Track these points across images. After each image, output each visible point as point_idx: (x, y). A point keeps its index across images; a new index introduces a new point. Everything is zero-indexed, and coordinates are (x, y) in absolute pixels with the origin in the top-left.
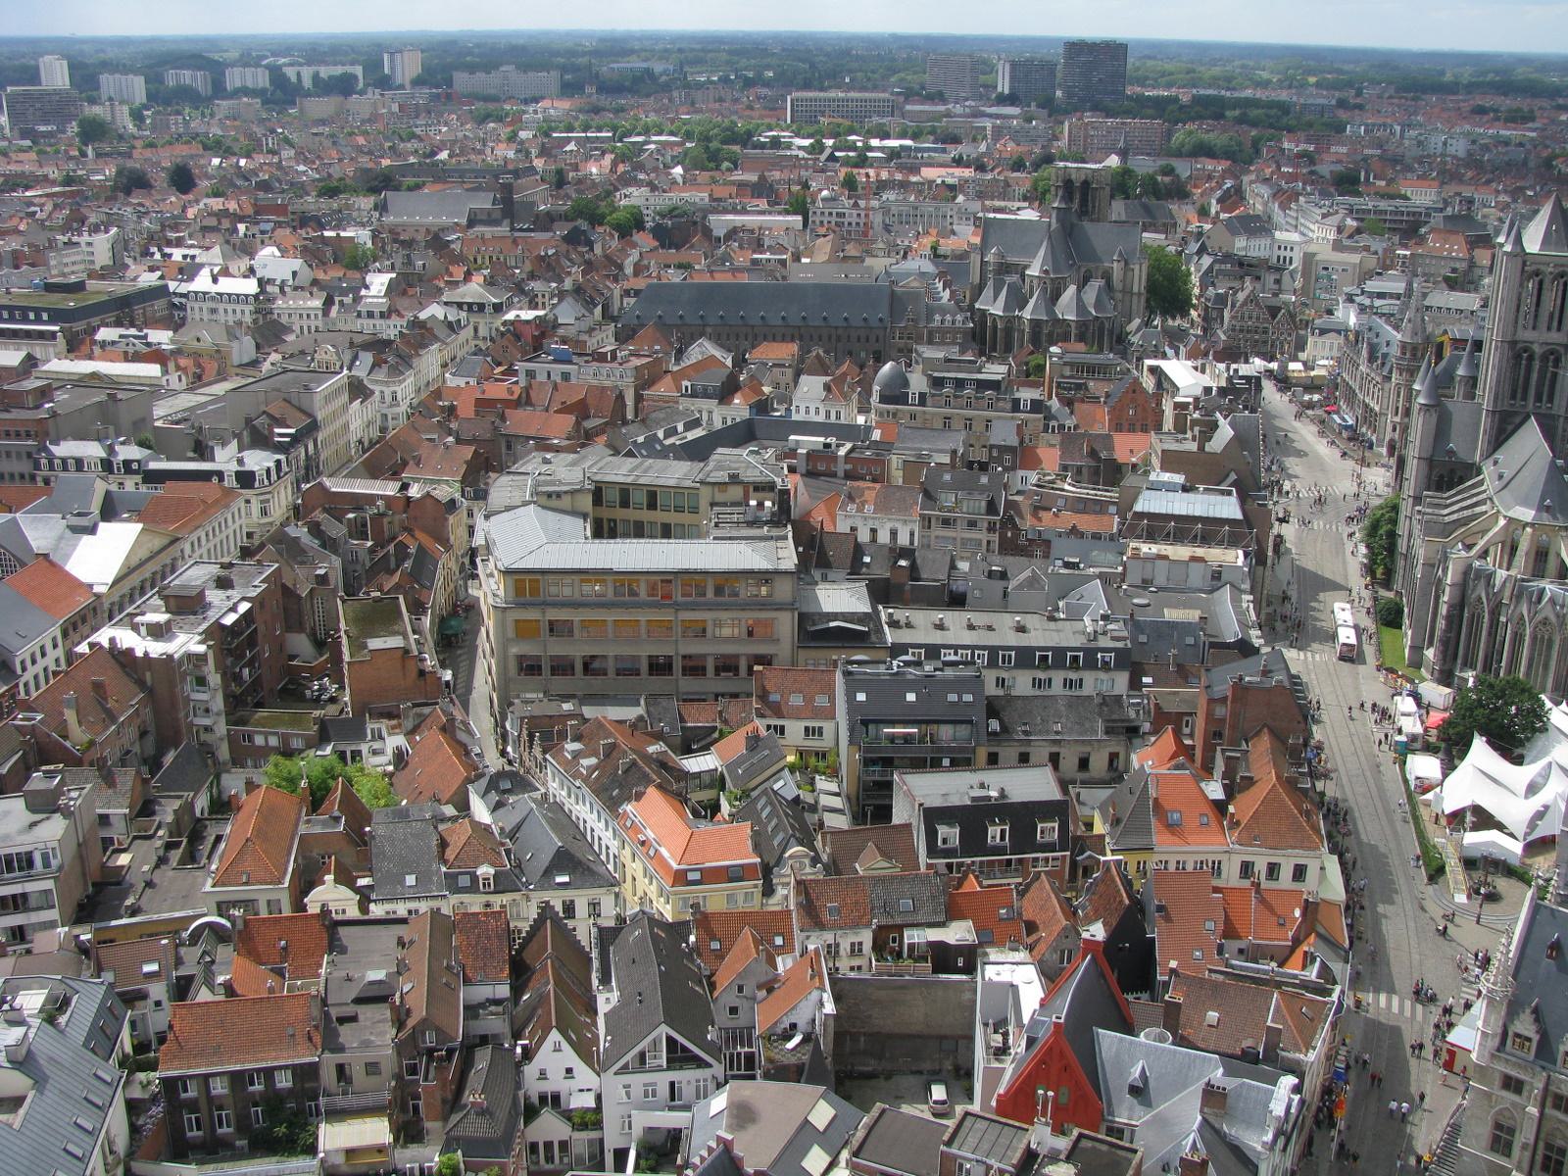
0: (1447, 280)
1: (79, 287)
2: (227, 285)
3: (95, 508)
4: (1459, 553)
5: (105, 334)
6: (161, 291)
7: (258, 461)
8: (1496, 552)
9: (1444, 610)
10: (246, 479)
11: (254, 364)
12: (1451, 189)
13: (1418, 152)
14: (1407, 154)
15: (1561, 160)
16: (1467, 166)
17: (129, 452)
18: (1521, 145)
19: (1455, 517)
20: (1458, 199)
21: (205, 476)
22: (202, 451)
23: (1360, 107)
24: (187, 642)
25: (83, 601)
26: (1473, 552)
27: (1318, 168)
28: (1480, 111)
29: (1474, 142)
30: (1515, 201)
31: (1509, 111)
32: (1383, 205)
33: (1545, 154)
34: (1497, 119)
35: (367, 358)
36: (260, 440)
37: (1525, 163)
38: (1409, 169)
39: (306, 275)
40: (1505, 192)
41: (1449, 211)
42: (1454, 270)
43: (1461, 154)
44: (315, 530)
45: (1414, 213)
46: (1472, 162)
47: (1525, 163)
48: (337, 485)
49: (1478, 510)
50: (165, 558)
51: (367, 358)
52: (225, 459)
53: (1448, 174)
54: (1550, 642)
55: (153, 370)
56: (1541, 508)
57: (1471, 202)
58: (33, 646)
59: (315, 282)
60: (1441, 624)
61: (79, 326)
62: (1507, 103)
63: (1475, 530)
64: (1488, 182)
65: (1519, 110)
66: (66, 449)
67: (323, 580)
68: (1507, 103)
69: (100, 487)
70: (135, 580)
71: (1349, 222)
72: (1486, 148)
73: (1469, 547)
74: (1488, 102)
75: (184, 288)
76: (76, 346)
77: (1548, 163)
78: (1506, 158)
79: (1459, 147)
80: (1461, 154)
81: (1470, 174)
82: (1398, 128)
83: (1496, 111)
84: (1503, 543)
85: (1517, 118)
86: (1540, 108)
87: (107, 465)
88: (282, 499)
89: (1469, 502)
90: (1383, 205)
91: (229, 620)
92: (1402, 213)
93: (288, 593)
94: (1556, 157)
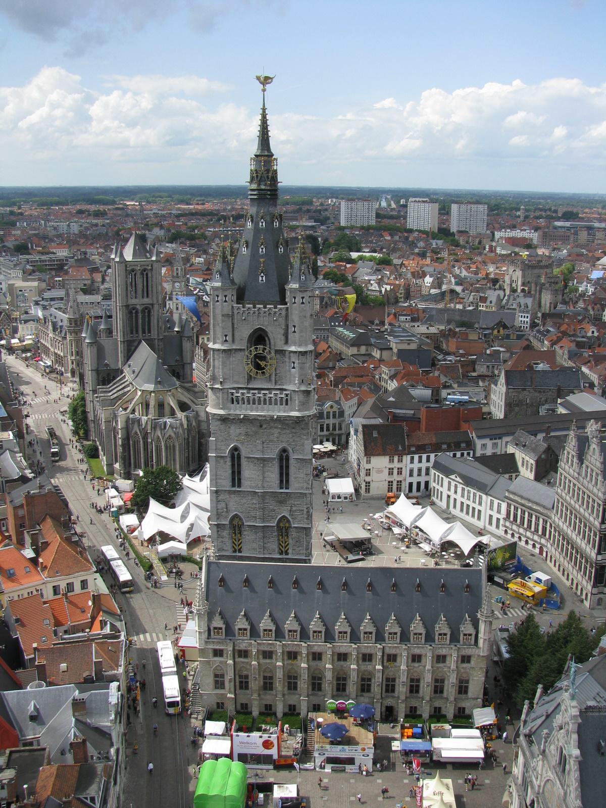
0: (82, 290)
4: (121, 412)
8: (139, 409)
9: (120, 442)
12: (75, 248)
13: (54, 233)
14: (50, 234)
15: (123, 231)
16: (80, 237)
18: (103, 226)
19: (116, 395)
20: (79, 253)
23: (21, 214)
26: (128, 411)
27: (6, 244)
28: (81, 212)
29: (81, 226)
30: (106, 251)
31: (95, 211)
32: (43, 257)
33: (116, 229)
34: (89, 215)
37: (107, 234)
38: (51, 241)
40: (101, 247)
41: (76, 258)
42: (85, 285)
43: (76, 232)
45: (60, 260)
46: (82, 235)
47: (107, 234)
49: (126, 390)
53: (71, 242)
54: (174, 446)
56: (158, 383)
57: (85, 253)
60: (120, 449)
62: (93, 208)
63: (127, 400)
64: (92, 244)
65: (99, 210)
68: (93, 208)
71: (28, 267)
72: (87, 229)
73: (125, 409)
74: (84, 207)
77: (117, 233)
78: (98, 232)
79: (75, 228)
80: (76, 232)
81: (82, 241)
82: (43, 222)
83: (89, 211)
84: (142, 403)
85: (98, 214)
86: (108, 209)
89: (121, 387)
90: (43, 257)
92: (54, 261)
94: (121, 230)
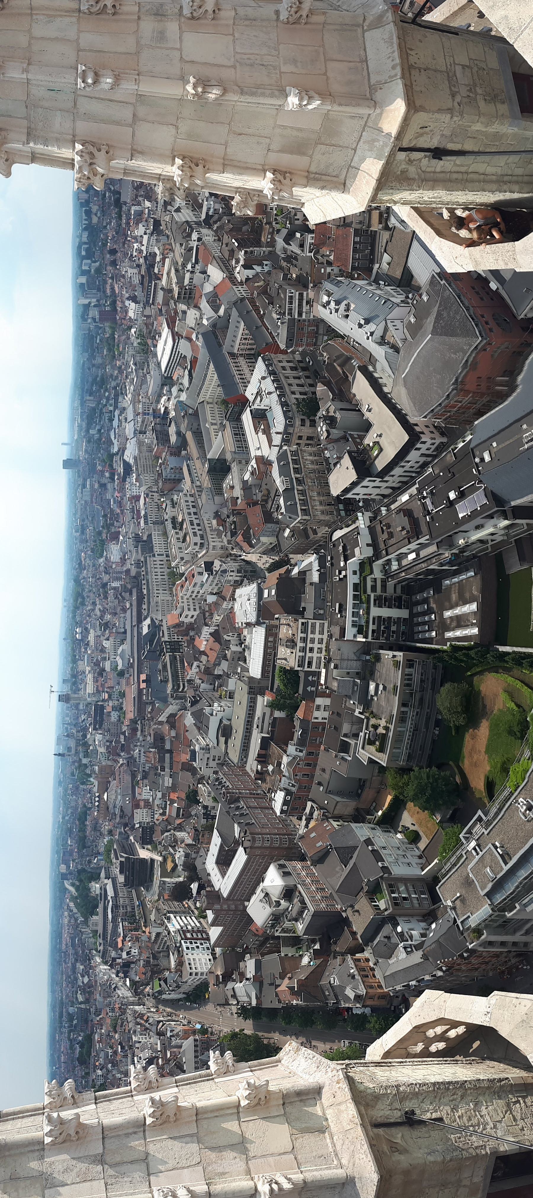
1: (143, 277)
2: (145, 242)
3: (203, 276)
5: (156, 271)
6: (146, 258)
7: (195, 236)
10: (199, 239)
11: (168, 237)
17: (189, 267)
21: (197, 249)
22: (191, 249)
24: (241, 255)
25: (227, 280)
35: (169, 208)
36: (189, 235)
39: (144, 223)
44: (215, 222)
48: (203, 216)
50: (219, 260)
51: (169, 208)
52: (194, 244)
55: (167, 260)
58: (237, 293)
59: (146, 221)
61: (153, 277)
66: (186, 282)
67: (229, 221)
69: (198, 274)
70: (223, 268)
75: (145, 252)
76: (159, 278)
87: (192, 272)
88: (205, 231)
91: (236, 244)
93: (231, 230)
